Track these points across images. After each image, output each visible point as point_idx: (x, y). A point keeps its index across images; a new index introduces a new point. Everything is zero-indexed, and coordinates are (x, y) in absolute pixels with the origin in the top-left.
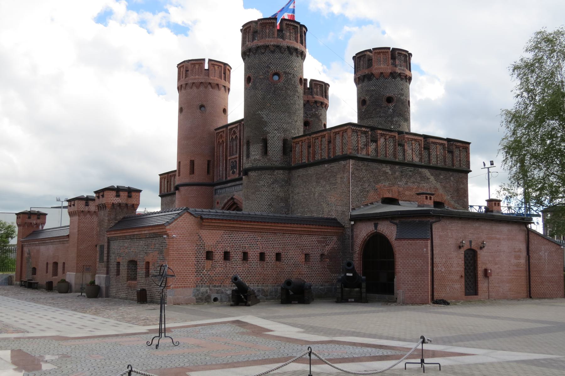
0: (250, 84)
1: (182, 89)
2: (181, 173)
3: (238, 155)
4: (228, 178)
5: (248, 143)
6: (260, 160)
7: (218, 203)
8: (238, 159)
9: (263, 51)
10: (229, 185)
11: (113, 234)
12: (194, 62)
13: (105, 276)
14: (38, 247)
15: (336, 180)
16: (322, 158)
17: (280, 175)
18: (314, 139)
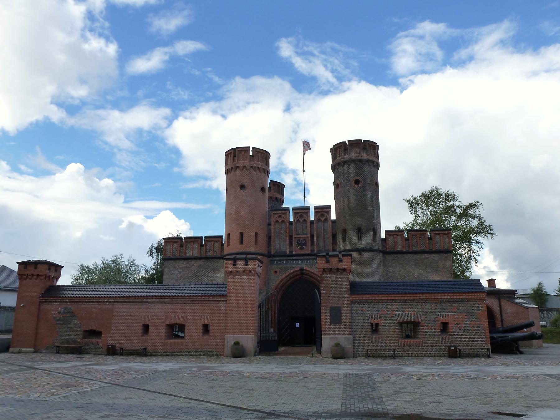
0: (360, 185)
1: (245, 169)
2: (231, 243)
3: (309, 235)
4: (294, 253)
5: (359, 230)
6: (372, 244)
7: (276, 272)
8: (309, 238)
9: (370, 163)
10: (294, 258)
11: (354, 298)
12: (258, 150)
13: (351, 337)
14: (108, 307)
15: (438, 265)
16: (421, 249)
17: (379, 257)
18: (411, 235)
